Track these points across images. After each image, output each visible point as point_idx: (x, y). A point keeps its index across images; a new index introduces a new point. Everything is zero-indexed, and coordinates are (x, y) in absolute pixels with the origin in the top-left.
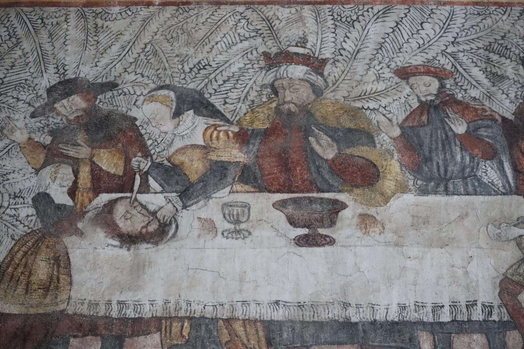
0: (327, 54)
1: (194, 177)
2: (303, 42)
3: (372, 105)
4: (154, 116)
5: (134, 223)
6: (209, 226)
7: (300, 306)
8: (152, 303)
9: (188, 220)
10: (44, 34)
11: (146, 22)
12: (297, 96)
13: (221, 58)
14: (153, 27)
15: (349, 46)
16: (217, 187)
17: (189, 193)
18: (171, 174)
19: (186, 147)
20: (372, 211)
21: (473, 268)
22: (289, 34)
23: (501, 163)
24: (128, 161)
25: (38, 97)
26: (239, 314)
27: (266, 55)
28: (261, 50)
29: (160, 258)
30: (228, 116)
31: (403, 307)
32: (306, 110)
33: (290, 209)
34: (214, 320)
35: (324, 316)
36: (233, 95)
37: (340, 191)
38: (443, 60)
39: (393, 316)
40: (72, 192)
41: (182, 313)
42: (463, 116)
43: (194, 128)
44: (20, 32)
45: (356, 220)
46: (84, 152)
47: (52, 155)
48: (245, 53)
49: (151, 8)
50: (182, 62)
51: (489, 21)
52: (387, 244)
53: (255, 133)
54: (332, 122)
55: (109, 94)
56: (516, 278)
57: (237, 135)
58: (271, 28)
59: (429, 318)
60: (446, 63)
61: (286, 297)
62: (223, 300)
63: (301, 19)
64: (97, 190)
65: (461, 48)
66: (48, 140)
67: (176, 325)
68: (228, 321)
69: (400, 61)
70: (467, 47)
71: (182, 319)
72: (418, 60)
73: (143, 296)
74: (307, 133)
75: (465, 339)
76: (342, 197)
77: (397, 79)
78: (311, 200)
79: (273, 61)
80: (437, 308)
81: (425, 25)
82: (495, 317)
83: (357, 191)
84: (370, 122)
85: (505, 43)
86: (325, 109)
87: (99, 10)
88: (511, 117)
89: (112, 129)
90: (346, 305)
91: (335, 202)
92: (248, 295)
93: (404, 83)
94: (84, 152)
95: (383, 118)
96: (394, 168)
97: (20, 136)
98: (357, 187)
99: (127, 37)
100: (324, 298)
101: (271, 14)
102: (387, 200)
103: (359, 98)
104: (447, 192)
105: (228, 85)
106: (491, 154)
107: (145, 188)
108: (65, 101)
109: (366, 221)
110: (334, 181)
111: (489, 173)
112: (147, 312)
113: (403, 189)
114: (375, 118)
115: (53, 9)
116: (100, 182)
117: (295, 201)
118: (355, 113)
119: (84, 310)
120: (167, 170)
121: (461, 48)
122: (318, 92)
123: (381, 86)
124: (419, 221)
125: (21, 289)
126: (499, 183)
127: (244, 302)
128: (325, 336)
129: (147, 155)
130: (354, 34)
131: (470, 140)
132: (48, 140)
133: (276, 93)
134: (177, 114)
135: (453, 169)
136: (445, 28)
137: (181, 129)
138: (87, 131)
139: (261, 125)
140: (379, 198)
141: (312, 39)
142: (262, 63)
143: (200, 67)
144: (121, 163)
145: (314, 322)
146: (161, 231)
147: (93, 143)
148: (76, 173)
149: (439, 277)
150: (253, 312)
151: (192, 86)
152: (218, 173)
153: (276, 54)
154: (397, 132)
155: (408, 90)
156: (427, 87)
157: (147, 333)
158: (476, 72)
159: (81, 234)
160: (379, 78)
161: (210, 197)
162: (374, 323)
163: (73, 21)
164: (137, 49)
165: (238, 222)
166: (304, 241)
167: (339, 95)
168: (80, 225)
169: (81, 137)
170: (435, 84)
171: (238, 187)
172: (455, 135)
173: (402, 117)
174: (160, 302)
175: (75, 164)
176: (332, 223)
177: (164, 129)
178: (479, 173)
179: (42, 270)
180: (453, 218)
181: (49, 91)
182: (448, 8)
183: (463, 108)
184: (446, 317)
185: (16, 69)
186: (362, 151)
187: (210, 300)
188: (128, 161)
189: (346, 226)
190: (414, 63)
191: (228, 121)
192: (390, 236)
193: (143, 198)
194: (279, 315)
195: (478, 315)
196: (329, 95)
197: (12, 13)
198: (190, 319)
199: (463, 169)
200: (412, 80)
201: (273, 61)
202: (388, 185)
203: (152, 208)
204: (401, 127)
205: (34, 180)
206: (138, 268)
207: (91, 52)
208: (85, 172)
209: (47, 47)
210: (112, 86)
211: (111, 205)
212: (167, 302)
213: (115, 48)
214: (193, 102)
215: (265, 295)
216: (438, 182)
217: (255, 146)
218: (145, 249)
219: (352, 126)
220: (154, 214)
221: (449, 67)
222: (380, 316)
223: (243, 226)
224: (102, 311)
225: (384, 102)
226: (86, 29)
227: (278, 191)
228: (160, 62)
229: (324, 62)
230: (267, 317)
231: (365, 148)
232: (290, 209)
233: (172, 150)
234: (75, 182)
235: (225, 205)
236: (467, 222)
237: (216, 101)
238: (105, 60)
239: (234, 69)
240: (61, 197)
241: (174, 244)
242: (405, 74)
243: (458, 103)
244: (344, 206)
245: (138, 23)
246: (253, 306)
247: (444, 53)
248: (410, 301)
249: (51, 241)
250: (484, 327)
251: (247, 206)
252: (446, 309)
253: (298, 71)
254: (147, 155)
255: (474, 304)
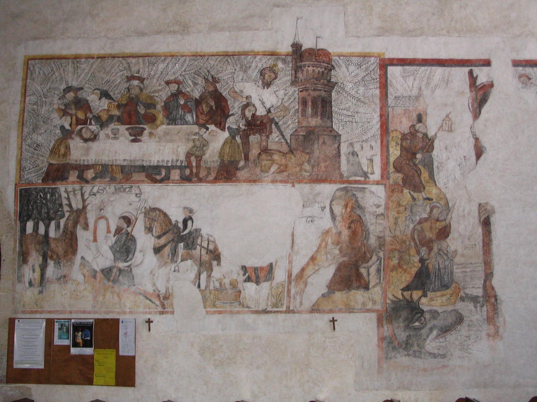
0: (145, 76)
1: (104, 120)
2: (138, 72)
3: (157, 95)
4: (93, 99)
5: (87, 135)
6: (108, 136)
7: (131, 161)
8: (92, 160)
9: (102, 134)
10: (62, 70)
11: (92, 64)
12: (135, 92)
13: (114, 78)
14: (94, 67)
15: (152, 73)
16: (111, 123)
17: (103, 125)
18: (98, 118)
19: (102, 110)
20: (153, 131)
21: (179, 149)
22: (134, 69)
23: (193, 114)
24: (86, 115)
25: (61, 93)
26: (114, 163)
27: (127, 77)
28: (126, 75)
29: (95, 146)
30: (115, 99)
31: (158, 161)
32: (137, 96)
33: (130, 130)
34: (108, 165)
35: (138, 163)
36: (117, 92)
37: (145, 124)
38: (180, 78)
39: (156, 164)
40: (71, 125)
41: (99, 163)
42: (184, 98)
43: (105, 103)
44: (55, 69)
45: (148, 134)
46: (73, 112)
47: (64, 113)
48: (122, 76)
49: (94, 60)
50: (102, 80)
51: (196, 63)
52: (156, 142)
53: (122, 105)
54: (144, 101)
55: (81, 92)
56: (191, 152)
57: (117, 105)
58: (129, 66)
59: (165, 165)
60: (181, 78)
61: (128, 158)
62: (111, 159)
63: (139, 63)
64: (77, 125)
65: (186, 73)
66: (63, 107)
67: (98, 167)
68: (112, 165)
69: (167, 78)
70: (188, 73)
71: (99, 165)
72: (172, 78)
73: (89, 158)
74: (137, 105)
75: (174, 171)
76: (145, 126)
77: (165, 85)
78: (136, 128)
79: (130, 78)
80: (168, 161)
81: (177, 65)
82: (183, 165)
83: (150, 124)
84: (155, 101)
85: (201, 71)
86: (143, 97)
87: (78, 60)
88: (198, 98)
89: (81, 104)
90: (143, 161)
91: (143, 128)
92: (117, 157)
93: (167, 86)
94: (73, 112)
95: (159, 100)
96: (160, 117)
97: (56, 106)
98: (149, 123)
99: (86, 71)
100: (138, 158)
101: (129, 61)
102: (157, 128)
103: (153, 92)
104: (175, 124)
105: (115, 88)
106: (190, 111)
107: (91, 124)
108: (68, 94)
109: (151, 134)
110: (143, 121)
111: (189, 117)
112: (90, 163)
113: (162, 123)
114: (157, 99)
115: (64, 60)
116: (79, 122)
117: (132, 128)
118: (151, 98)
119: (73, 162)
120: (97, 118)
121: (186, 73)
122: (141, 90)
123: (160, 88)
124: (166, 134)
125: (57, 156)
126: (191, 121)
127: (116, 160)
128: (137, 170)
129: (91, 113)
130: (154, 69)
131: (184, 107)
132: (63, 107)
133: (129, 91)
134: (100, 99)
135: (178, 116)
136: (182, 66)
137: (101, 104)
138: (75, 104)
139: (124, 102)
140: (155, 127)
141: (141, 70)
142: (126, 80)
143: (108, 82)
144: (84, 115)
145: (134, 166)
146: (94, 138)
147: (77, 109)
148: (71, 119)
149: (170, 152)
150: (118, 163)
151: (105, 89)
152: (111, 118)
153: (131, 76)
154: (163, 104)
155: (168, 89)
156: (174, 87)
157: (90, 169)
158: (190, 82)
159: (72, 138)
160: (160, 85)
161: (108, 127)
162: (150, 166)
163: (70, 65)
164: (89, 75)
165: (115, 135)
166: (133, 141)
167: (148, 90)
168: (73, 136)
169: (73, 107)
170: (177, 86)
171: (116, 123)
172: (180, 105)
173: (165, 99)
174: (94, 160)
175: (71, 115)
176: (142, 135)
177: (97, 104)
178: (186, 118)
179: (62, 150)
180: (176, 132)
181: (64, 90)
182: (184, 58)
183: (184, 94)
184: (170, 164)
185: (54, 82)
186: (152, 111)
187: (107, 159)
188: (86, 115)
189: (145, 137)
190: (171, 79)
191: (114, 101)
192: (157, 139)
193: (90, 127)
194: (125, 163)
195: (179, 164)
196: (144, 91)
197: (52, 61)
198: (102, 165)
199: (181, 116)
200: (170, 85)
201: (130, 78)
202: (158, 122)
203: (92, 130)
204: (165, 102)
205: (60, 121)
206: (88, 150)
207: (76, 76)
208: (74, 118)
209: (63, 75)
210: (82, 89)
211: (82, 129)
212: (96, 160)
213: (83, 75)
214: (105, 94)
215: (122, 157)
216: (172, 120)
217: (121, 110)
218: (90, 143)
219: (150, 102)
220: (93, 132)
221: (181, 80)
222: (152, 164)
223: (117, 136)
224: (78, 163)
225: (161, 93)
226: (74, 68)
227: (127, 125)
228: (96, 80)
229: (144, 79)
230: (122, 164)
231: (153, 110)
232: (130, 130)
233: (98, 111)
234: (71, 122)
235: (112, 129)
236: (180, 134)
237: (111, 94)
238: (80, 80)
239: (117, 82)
240: (67, 127)
241: (98, 142)
242: (168, 83)
243: (183, 93)
244: (145, 129)
245: (89, 66)
246: (118, 161)
247: (181, 75)
248: (160, 159)
249: (64, 141)
250: (180, 168)
251: (118, 130)
252: (170, 162)
253: (136, 83)
254: (91, 113)
255: (178, 160)
